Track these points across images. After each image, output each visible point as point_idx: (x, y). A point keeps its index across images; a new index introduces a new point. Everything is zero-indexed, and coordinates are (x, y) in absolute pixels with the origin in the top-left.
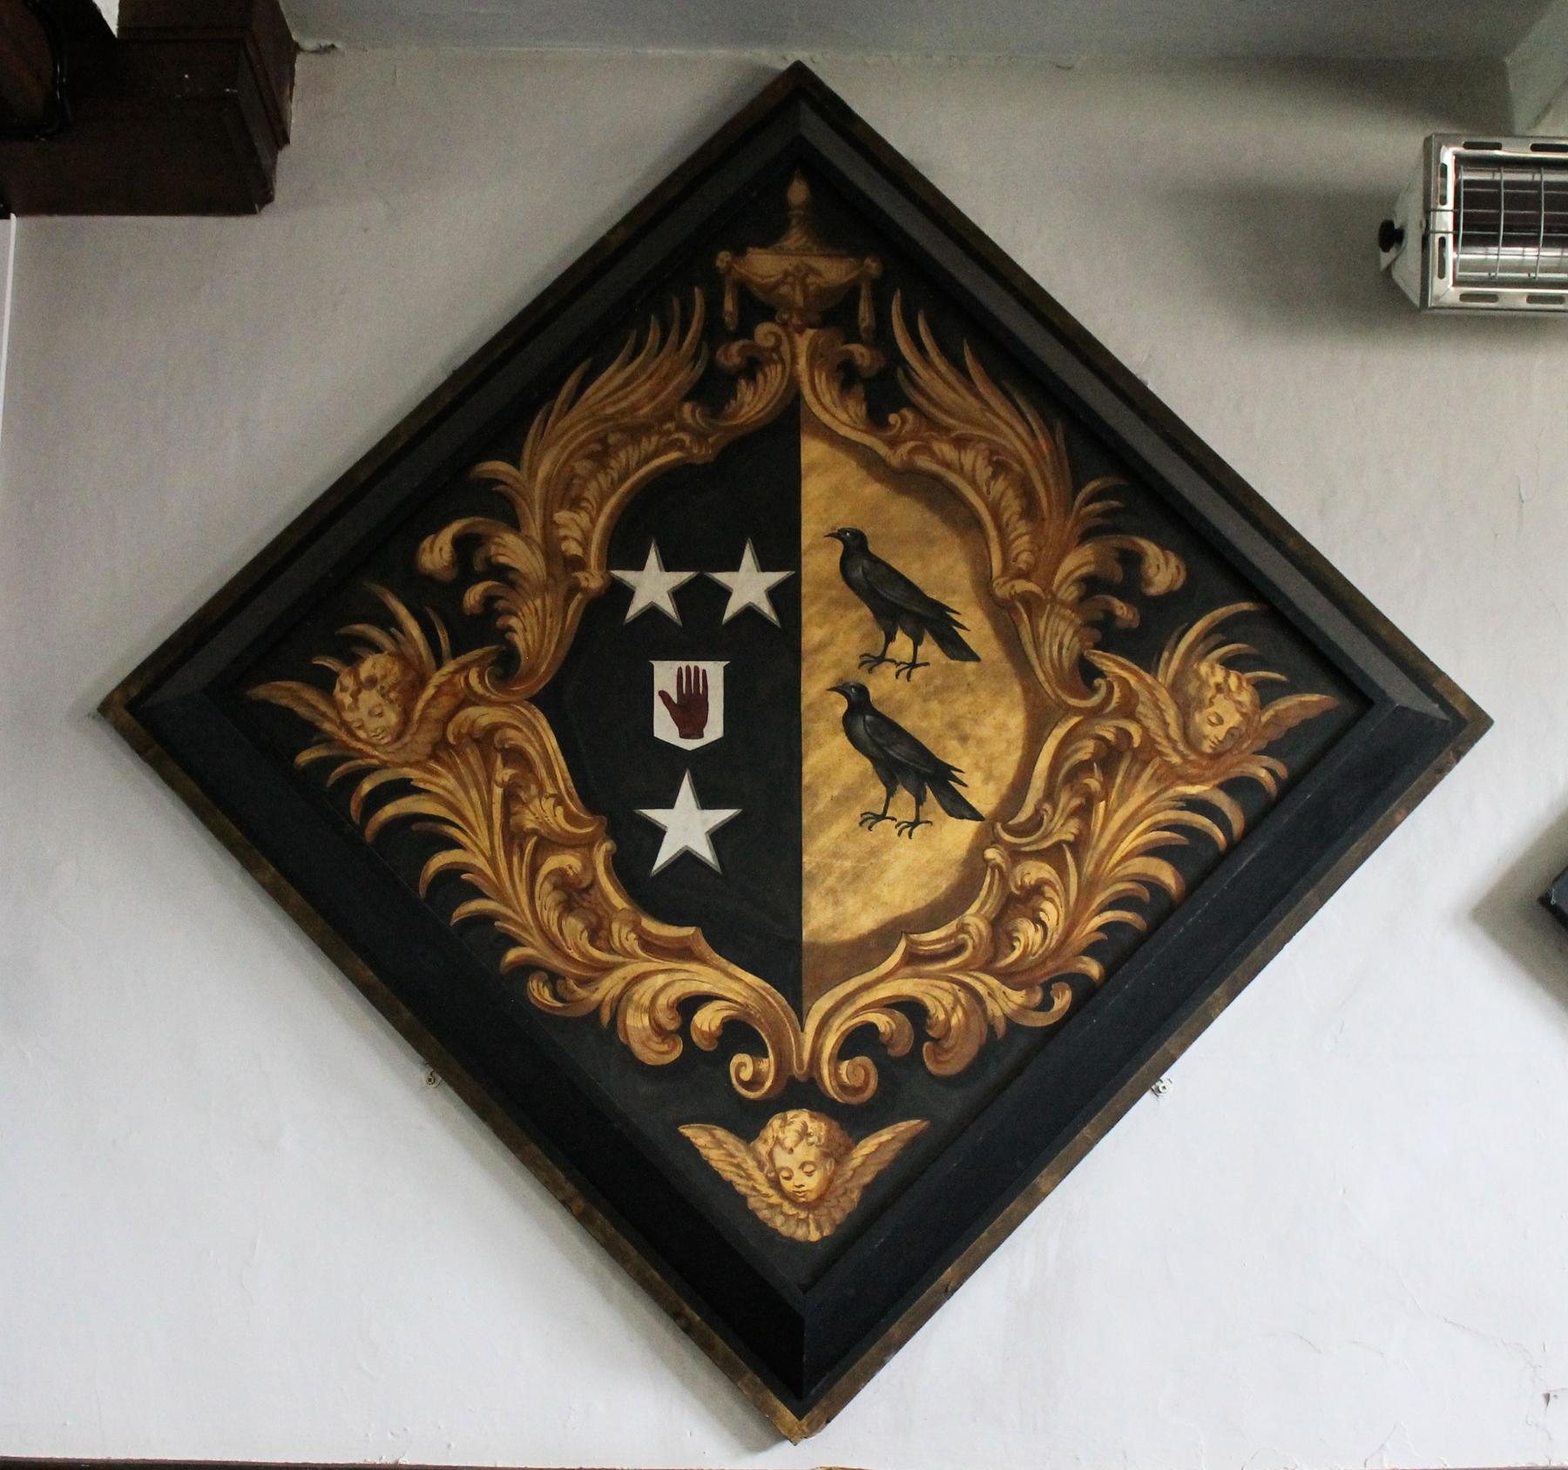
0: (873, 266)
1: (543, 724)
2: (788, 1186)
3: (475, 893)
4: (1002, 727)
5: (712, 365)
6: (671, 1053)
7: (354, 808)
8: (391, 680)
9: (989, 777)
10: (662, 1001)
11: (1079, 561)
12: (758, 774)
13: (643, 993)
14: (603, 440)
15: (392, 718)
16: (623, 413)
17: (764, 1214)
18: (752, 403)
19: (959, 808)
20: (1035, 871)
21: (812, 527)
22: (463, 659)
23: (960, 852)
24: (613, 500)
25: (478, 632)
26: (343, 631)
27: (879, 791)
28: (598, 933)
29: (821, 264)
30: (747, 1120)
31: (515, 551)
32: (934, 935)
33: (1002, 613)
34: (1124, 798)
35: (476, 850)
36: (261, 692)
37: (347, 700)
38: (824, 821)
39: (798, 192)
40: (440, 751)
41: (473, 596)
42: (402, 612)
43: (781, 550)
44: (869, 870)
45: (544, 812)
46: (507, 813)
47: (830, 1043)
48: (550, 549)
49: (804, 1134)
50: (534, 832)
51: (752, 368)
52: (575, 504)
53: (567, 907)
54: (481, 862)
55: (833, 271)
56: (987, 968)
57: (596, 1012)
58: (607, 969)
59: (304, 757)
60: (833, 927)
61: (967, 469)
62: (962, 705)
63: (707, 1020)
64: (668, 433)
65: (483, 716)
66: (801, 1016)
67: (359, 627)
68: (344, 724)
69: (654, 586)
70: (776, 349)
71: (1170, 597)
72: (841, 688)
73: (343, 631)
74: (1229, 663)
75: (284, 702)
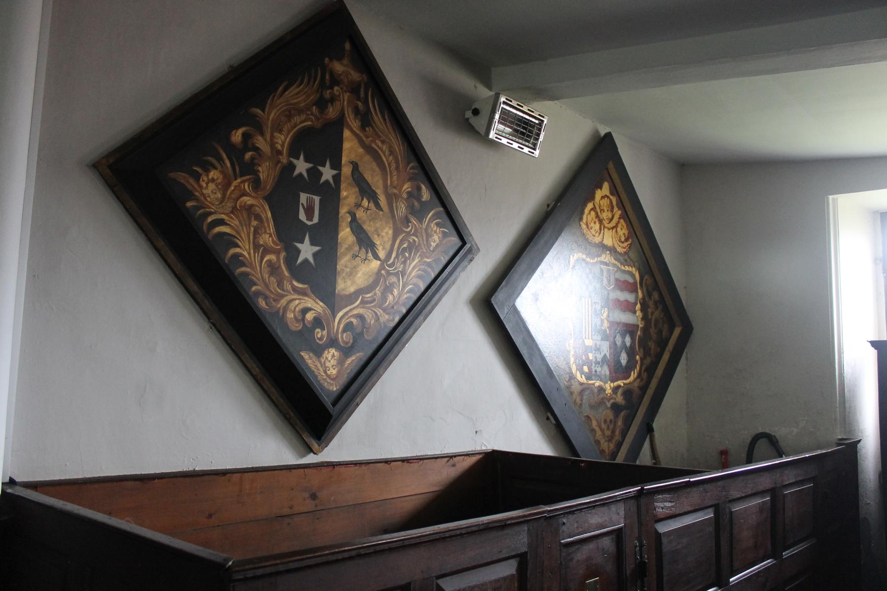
0: (365, 77)
1: (267, 208)
2: (328, 372)
3: (243, 264)
4: (387, 233)
5: (321, 96)
6: (300, 327)
7: (205, 227)
8: (219, 181)
9: (384, 248)
10: (297, 309)
11: (407, 187)
13: (292, 306)
14: (290, 111)
15: (219, 195)
16: (296, 103)
17: (322, 382)
18: (332, 112)
19: (376, 257)
20: (393, 279)
21: (344, 160)
22: (244, 178)
23: (376, 270)
24: (291, 134)
25: (248, 169)
26: (205, 158)
27: (357, 248)
28: (280, 284)
29: (352, 72)
30: (318, 351)
31: (261, 142)
32: (368, 295)
33: (390, 198)
34: (413, 260)
35: (244, 249)
36: (172, 175)
37: (205, 185)
38: (345, 254)
39: (347, 46)
40: (234, 210)
41: (248, 155)
42: (224, 156)
44: (355, 273)
45: (268, 238)
46: (255, 238)
47: (342, 326)
48: (272, 145)
49: (333, 356)
50: (262, 245)
51: (332, 100)
52: (280, 131)
53: (271, 274)
54: (245, 253)
55: (355, 76)
56: (380, 307)
57: (278, 312)
58: (283, 296)
59: (189, 204)
60: (343, 290)
61: (383, 149)
62: (378, 224)
63: (309, 316)
64: (307, 115)
65: (248, 200)
66: (334, 317)
67: (210, 158)
68: (203, 194)
69: (302, 166)
70: (339, 96)
71: (425, 202)
72: (349, 213)
73: (205, 158)
74: (437, 224)
75: (182, 181)
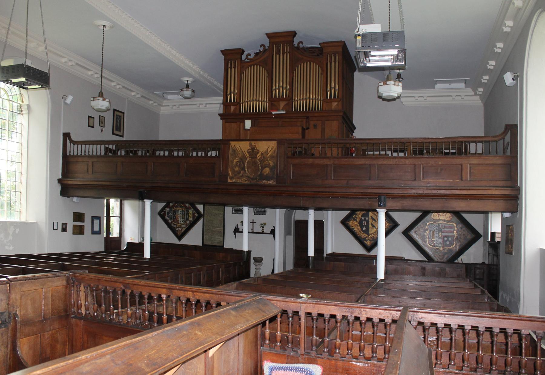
12: (367, 226)
25: (356, 220)
35: (356, 229)
43: (368, 217)
69: (363, 218)
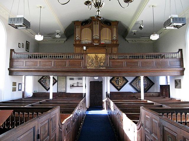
12: (118, 82)
35: (114, 83)
44: (120, 84)
